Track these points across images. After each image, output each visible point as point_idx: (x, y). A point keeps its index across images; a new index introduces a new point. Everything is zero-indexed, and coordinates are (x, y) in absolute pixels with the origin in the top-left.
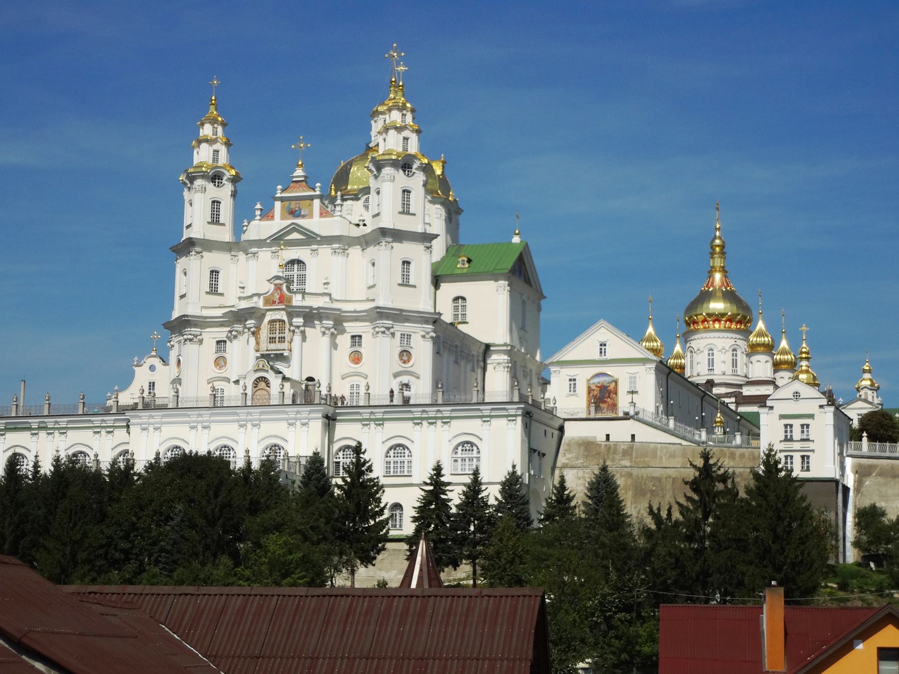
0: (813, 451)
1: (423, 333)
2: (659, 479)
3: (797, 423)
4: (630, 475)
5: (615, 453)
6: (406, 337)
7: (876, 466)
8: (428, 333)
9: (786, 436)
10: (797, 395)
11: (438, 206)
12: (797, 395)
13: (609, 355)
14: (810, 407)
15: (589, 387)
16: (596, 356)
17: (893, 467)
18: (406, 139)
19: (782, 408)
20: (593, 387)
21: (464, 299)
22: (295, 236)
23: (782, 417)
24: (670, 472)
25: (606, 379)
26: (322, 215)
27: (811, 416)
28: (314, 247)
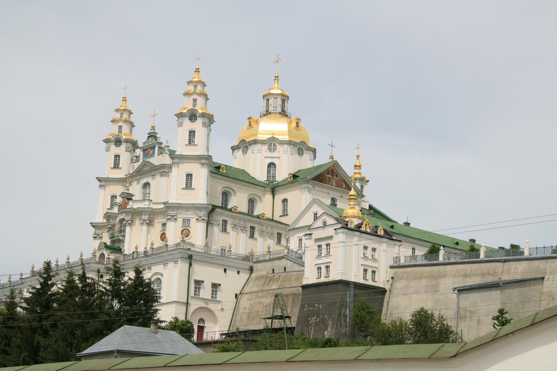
0: (330, 262)
1: (197, 217)
3: (323, 244)
6: (186, 222)
8: (200, 217)
10: (325, 224)
12: (325, 224)
14: (329, 231)
18: (195, 100)
19: (317, 234)
21: (287, 199)
22: (146, 168)
23: (317, 240)
26: (159, 154)
27: (331, 237)
28: (154, 173)
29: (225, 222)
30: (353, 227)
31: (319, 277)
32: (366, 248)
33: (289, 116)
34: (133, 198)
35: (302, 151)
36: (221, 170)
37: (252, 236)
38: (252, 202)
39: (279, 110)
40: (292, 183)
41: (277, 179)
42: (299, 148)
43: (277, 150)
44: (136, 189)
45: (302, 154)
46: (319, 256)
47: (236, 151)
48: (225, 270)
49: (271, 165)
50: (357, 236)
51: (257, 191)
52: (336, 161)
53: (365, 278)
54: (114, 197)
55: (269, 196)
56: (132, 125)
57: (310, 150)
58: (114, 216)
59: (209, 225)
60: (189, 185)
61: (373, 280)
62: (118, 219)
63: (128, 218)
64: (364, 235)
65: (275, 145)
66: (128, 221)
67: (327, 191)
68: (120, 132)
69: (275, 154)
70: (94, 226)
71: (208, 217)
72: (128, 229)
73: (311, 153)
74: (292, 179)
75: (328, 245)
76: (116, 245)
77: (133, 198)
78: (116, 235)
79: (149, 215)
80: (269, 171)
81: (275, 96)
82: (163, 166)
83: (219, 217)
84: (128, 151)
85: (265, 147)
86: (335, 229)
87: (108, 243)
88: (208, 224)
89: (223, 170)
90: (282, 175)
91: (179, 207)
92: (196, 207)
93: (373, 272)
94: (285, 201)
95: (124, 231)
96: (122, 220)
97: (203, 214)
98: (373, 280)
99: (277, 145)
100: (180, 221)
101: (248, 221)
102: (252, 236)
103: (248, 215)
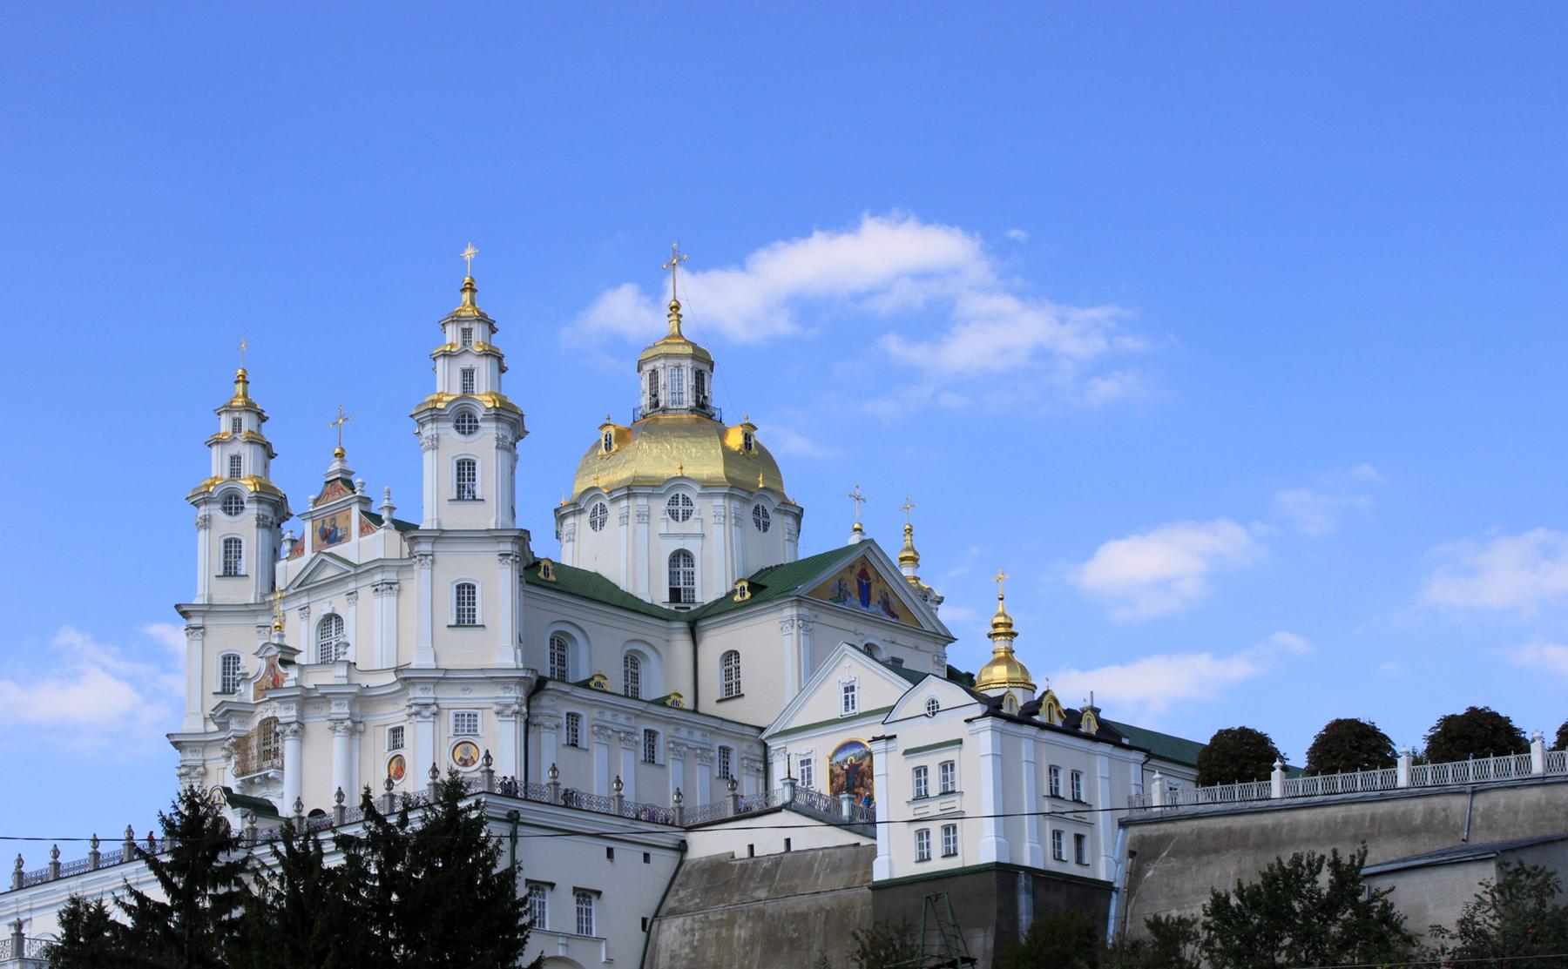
1: (496, 708)
2: (803, 917)
3: (932, 761)
4: (761, 915)
5: (750, 878)
6: (466, 721)
7: (1163, 840)
8: (508, 706)
9: (919, 791)
10: (933, 708)
11: (719, 501)
12: (933, 708)
13: (861, 707)
15: (831, 772)
16: (838, 711)
17: (1200, 835)
19: (912, 735)
20: (838, 770)
21: (736, 653)
22: (329, 573)
24: (824, 900)
25: (857, 751)
29: (573, 718)
30: (1015, 712)
31: (923, 858)
32: (1054, 770)
33: (717, 417)
34: (298, 659)
35: (766, 515)
36: (541, 575)
37: (650, 759)
38: (632, 661)
39: (689, 400)
40: (744, 605)
41: (698, 599)
42: (757, 507)
43: (694, 516)
44: (301, 634)
45: (766, 527)
46: (921, 796)
47: (569, 521)
48: (610, 852)
49: (681, 558)
50: (1028, 737)
51: (649, 630)
52: (872, 541)
53: (1058, 858)
54: (230, 661)
55: (682, 644)
56: (269, 452)
57: (786, 513)
58: (244, 712)
59: (532, 728)
60: (465, 616)
61: (1079, 861)
62: (258, 719)
63: (286, 714)
64: (1047, 735)
65: (686, 500)
66: (288, 724)
67: (851, 625)
68: (235, 472)
69: (691, 526)
70: (176, 744)
71: (528, 707)
72: (289, 747)
73: (790, 520)
74: (748, 595)
75: (947, 767)
76: (258, 793)
77: (297, 659)
78: (254, 764)
79: (351, 705)
80: (673, 576)
81: (676, 362)
82: (380, 565)
83: (554, 707)
84: (265, 526)
85: (660, 506)
86: (968, 721)
87: (236, 791)
88: (529, 725)
89: (546, 574)
90: (711, 584)
91: (442, 678)
92: (492, 679)
93: (1079, 838)
94: (731, 657)
95: (277, 753)
96: (269, 725)
97: (514, 695)
98: (1079, 861)
99: (693, 498)
100: (449, 720)
101: (637, 716)
102: (650, 759)
103: (626, 696)
